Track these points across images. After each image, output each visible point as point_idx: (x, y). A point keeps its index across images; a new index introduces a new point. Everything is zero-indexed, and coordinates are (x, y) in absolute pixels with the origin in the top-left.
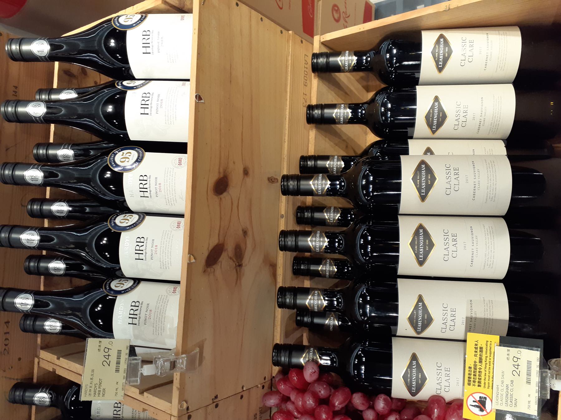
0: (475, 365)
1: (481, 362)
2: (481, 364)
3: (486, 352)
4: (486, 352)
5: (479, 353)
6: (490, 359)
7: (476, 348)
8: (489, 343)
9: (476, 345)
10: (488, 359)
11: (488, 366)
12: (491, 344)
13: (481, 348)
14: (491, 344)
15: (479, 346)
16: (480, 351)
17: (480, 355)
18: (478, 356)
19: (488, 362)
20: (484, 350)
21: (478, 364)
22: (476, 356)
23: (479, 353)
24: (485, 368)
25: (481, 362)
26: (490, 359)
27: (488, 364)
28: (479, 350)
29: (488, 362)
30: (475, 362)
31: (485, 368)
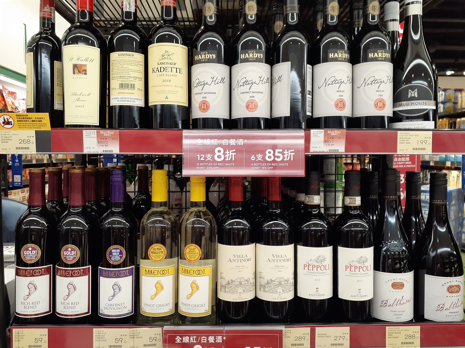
0: (30, 118)
1: (33, 121)
2: (31, 121)
3: (40, 124)
4: (40, 124)
5: (38, 120)
6: (36, 126)
7: (40, 118)
8: (45, 125)
9: (42, 118)
10: (36, 125)
11: (31, 125)
12: (45, 126)
13: (41, 121)
14: (45, 126)
15: (42, 119)
16: (39, 121)
17: (37, 121)
18: (36, 120)
19: (34, 125)
20: (40, 123)
21: (31, 120)
22: (36, 118)
23: (38, 120)
24: (30, 124)
25: (33, 121)
26: (36, 126)
27: (33, 125)
28: (40, 120)
29: (34, 125)
30: (32, 118)
31: (30, 124)
